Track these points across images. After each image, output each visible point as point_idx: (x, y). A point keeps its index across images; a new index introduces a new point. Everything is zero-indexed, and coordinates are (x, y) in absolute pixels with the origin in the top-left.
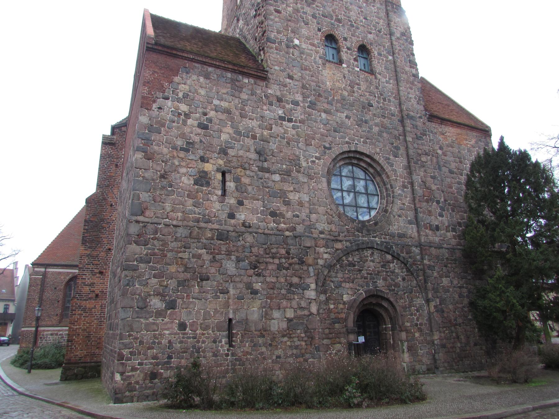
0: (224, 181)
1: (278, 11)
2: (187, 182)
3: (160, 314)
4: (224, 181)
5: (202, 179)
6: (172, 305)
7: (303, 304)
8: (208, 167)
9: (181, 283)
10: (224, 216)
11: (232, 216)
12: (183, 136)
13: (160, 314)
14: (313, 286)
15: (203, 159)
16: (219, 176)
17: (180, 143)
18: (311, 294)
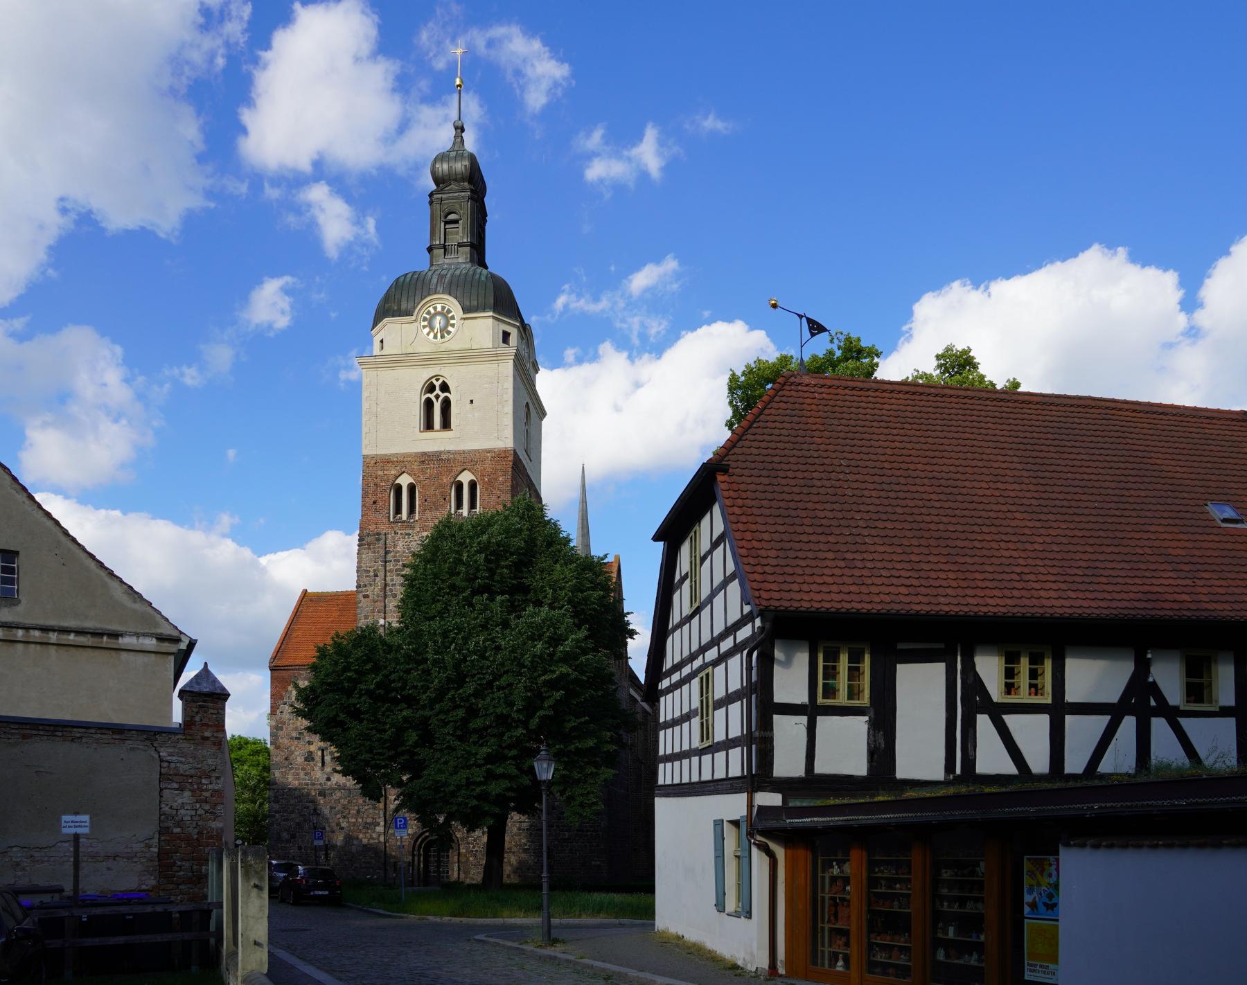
0: (323, 756)
1: (366, 596)
2: (300, 760)
3: (288, 841)
4: (323, 756)
5: (309, 757)
6: (293, 836)
7: (374, 836)
8: (313, 748)
9: (298, 824)
10: (323, 781)
11: (329, 779)
12: (296, 729)
13: (288, 841)
14: (382, 824)
15: (310, 743)
16: (320, 753)
17: (294, 734)
18: (380, 829)
